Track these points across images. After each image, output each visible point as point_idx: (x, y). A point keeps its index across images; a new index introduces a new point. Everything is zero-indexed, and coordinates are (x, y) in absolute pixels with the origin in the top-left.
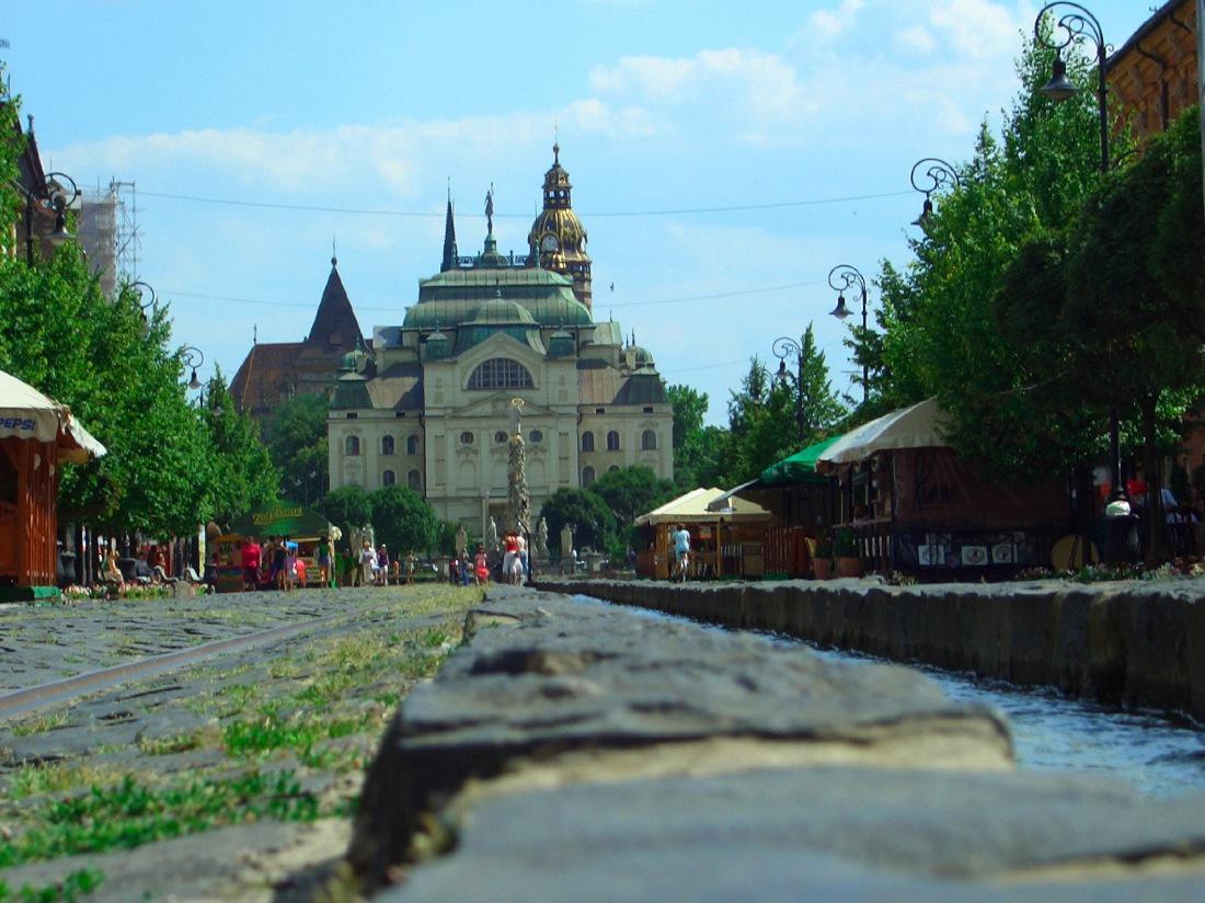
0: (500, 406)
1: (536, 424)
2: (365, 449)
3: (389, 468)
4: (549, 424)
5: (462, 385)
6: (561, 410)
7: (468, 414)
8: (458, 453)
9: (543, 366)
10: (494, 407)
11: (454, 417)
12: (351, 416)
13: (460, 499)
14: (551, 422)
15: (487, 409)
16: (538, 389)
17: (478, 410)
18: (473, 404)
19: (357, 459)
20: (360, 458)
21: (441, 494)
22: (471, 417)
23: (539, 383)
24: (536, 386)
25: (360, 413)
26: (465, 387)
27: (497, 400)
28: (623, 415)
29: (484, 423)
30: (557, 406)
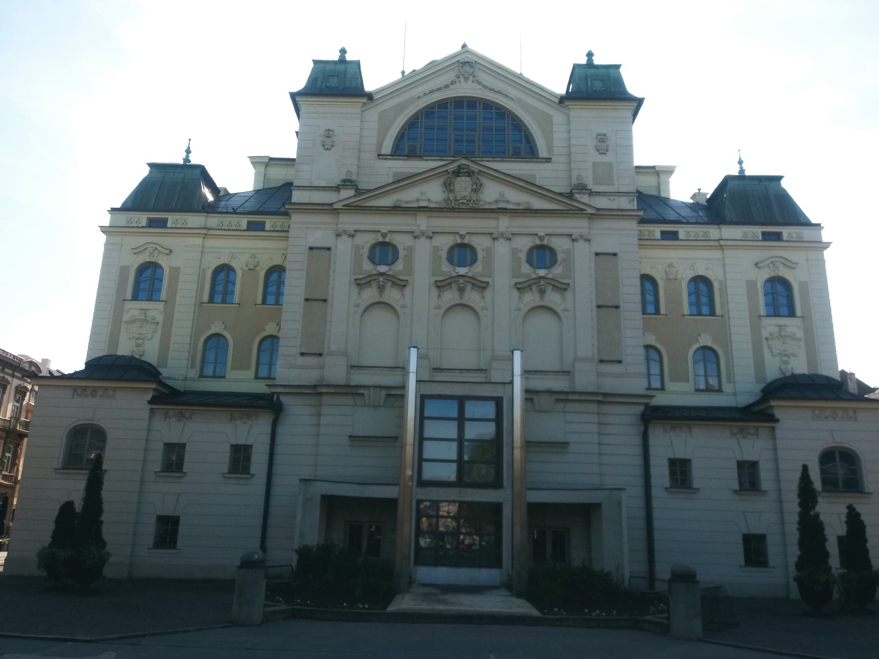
0: (463, 185)
1: (542, 226)
2: (173, 291)
3: (216, 328)
4: (575, 232)
5: (380, 145)
6: (602, 203)
7: (387, 201)
8: (361, 284)
9: (558, 117)
10: (448, 186)
11: (351, 208)
12: (152, 223)
13: (351, 391)
14: (577, 226)
15: (434, 193)
16: (548, 160)
17: (409, 196)
18: (403, 182)
19: (155, 310)
20: (160, 306)
21: (309, 377)
22: (396, 209)
23: (550, 148)
24: (543, 152)
25: (172, 218)
26: (387, 148)
27: (457, 173)
28: (720, 245)
29: (423, 223)
30: (591, 193)
